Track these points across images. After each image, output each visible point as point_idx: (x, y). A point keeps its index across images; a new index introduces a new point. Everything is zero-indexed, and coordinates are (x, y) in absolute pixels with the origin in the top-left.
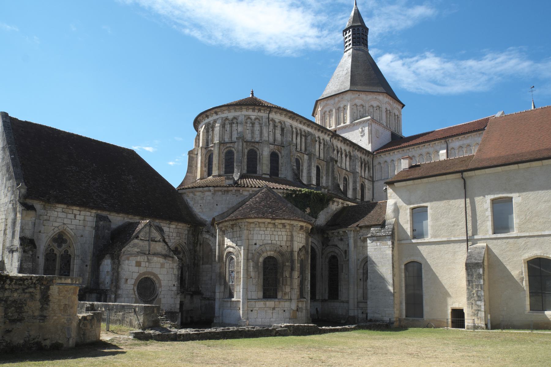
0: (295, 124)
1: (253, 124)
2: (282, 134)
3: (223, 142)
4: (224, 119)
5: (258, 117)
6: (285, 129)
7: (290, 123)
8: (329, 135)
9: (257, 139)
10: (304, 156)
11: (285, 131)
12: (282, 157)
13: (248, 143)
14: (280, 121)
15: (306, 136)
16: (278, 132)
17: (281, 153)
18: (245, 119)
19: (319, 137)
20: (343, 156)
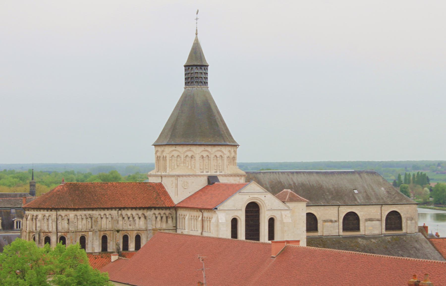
0: (79, 213)
1: (48, 219)
2: (68, 223)
3: (32, 231)
4: (32, 215)
5: (50, 215)
6: (70, 220)
7: (75, 214)
8: (115, 210)
9: (50, 230)
10: (88, 234)
11: (70, 221)
12: (68, 239)
13: (45, 233)
14: (65, 215)
15: (91, 218)
16: (66, 222)
17: (67, 237)
18: (43, 216)
19: (105, 214)
20: (136, 218)
